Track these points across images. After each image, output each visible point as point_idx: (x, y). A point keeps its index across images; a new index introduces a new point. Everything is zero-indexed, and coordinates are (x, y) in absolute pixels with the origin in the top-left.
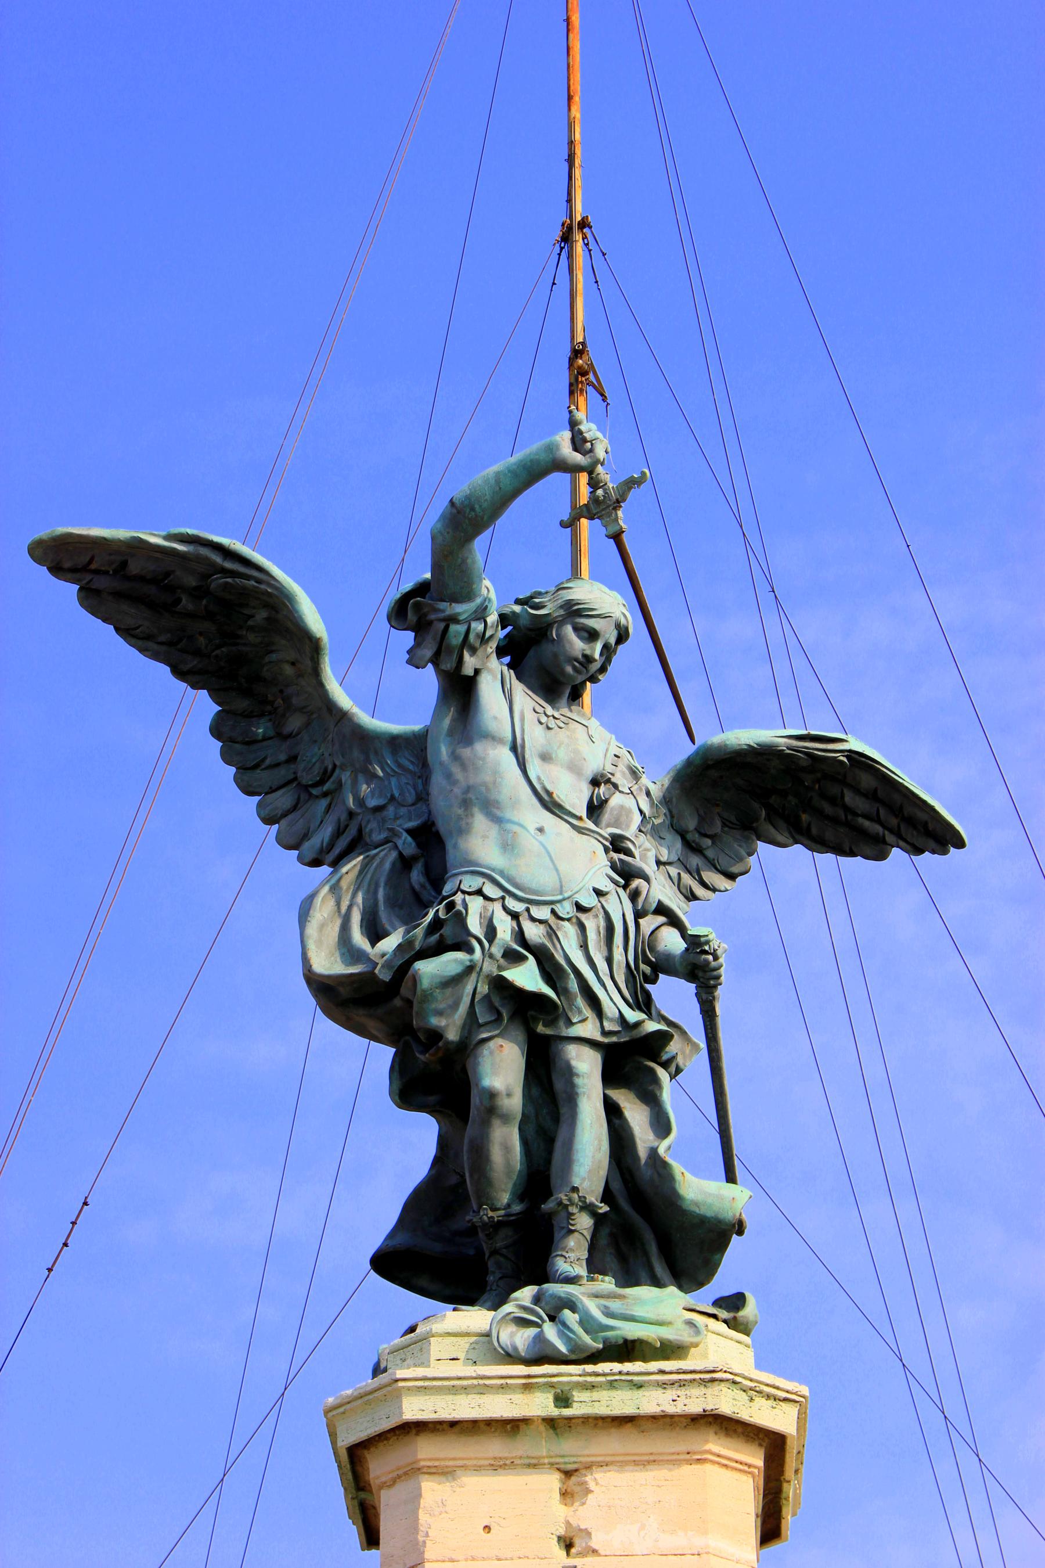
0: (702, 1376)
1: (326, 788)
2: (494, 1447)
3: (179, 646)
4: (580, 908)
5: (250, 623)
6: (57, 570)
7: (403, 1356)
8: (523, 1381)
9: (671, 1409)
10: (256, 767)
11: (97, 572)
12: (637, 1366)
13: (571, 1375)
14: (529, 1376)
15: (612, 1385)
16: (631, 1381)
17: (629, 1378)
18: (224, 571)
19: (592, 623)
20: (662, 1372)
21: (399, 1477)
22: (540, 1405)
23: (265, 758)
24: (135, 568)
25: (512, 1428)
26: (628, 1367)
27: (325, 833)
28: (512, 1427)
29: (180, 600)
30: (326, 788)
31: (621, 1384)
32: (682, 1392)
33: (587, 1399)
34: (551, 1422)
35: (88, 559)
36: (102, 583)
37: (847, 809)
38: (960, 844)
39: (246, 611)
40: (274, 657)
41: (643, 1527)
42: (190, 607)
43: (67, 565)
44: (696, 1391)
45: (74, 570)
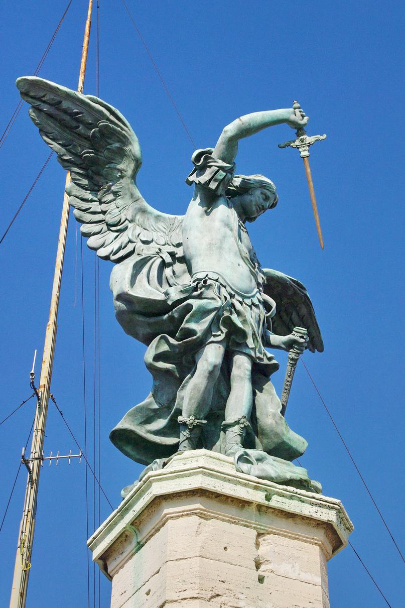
0: (330, 505)
1: (118, 228)
2: (232, 511)
3: (68, 148)
4: (253, 304)
5: (109, 147)
6: (25, 94)
7: (185, 462)
8: (256, 484)
9: (315, 516)
10: (84, 211)
11: (44, 102)
12: (303, 492)
14: (258, 483)
15: (291, 497)
16: (300, 498)
17: (300, 496)
18: (108, 119)
19: (268, 193)
20: (314, 498)
21: (182, 516)
22: (259, 497)
23: (90, 208)
24: (65, 104)
25: (242, 506)
26: (299, 491)
27: (115, 246)
28: (243, 504)
29: (78, 127)
30: (118, 228)
31: (296, 498)
32: (319, 509)
33: (280, 501)
34: (260, 507)
35: (42, 95)
36: (45, 108)
37: (291, 320)
38: (321, 350)
39: (109, 141)
40: (112, 165)
41: (293, 566)
42: (83, 131)
43: (32, 94)
44: (325, 511)
45: (32, 97)
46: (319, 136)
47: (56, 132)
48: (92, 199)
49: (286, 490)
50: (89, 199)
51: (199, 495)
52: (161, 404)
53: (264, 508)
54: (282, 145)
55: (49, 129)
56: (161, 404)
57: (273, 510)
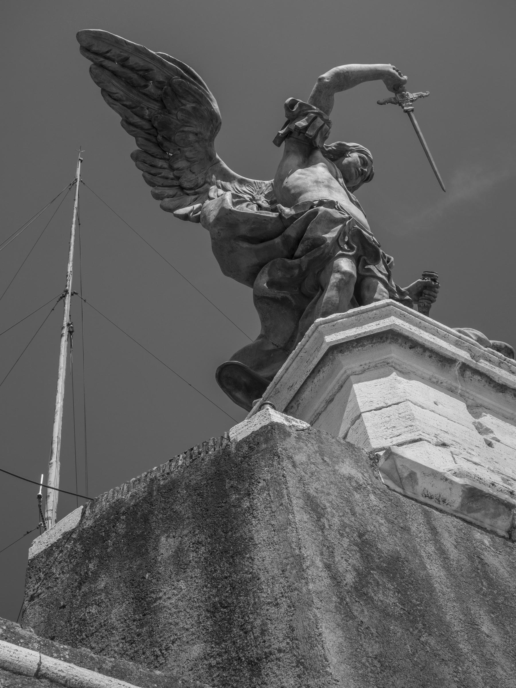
13: (480, 348)
18: (182, 77)
22: (463, 355)
46: (421, 93)
47: (122, 93)
48: (162, 166)
49: (493, 354)
50: (159, 166)
51: (389, 341)
52: (275, 345)
53: (468, 373)
54: (382, 101)
55: (114, 90)
56: (275, 345)
57: (479, 378)
